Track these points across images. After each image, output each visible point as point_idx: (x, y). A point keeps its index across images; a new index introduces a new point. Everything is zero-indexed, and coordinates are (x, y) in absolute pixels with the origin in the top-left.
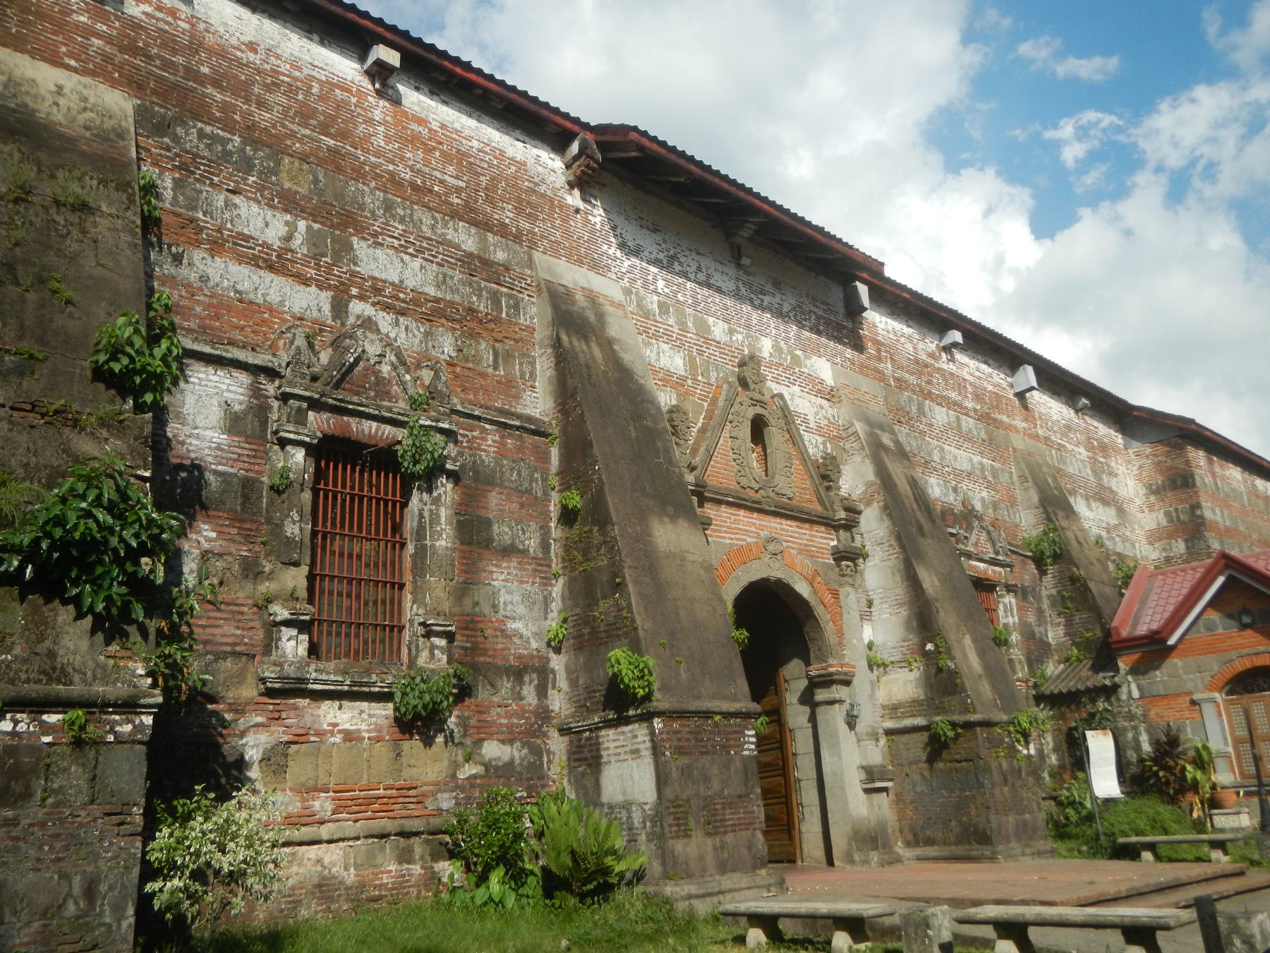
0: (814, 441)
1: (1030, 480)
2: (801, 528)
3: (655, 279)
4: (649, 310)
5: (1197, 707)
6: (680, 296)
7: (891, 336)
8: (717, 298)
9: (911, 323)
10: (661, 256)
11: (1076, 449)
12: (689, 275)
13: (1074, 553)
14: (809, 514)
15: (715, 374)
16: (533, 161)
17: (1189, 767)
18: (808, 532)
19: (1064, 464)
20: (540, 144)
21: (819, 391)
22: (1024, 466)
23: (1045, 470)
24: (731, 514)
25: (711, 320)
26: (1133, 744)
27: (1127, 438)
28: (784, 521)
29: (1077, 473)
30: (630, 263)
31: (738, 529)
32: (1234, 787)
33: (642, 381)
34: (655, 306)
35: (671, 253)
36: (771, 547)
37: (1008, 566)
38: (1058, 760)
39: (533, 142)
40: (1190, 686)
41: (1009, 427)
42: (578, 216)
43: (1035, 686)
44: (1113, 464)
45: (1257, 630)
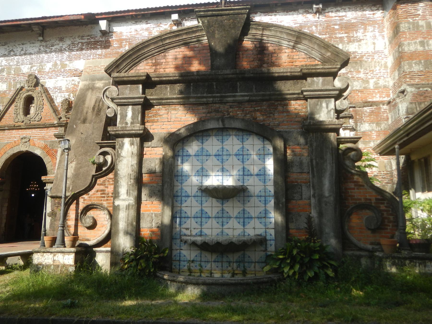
0: (63, 96)
2: (42, 130)
6: (11, 64)
8: (28, 57)
9: (149, 22)
15: (19, 85)
28: (33, 130)
31: (12, 137)
35: (11, 49)
36: (24, 140)
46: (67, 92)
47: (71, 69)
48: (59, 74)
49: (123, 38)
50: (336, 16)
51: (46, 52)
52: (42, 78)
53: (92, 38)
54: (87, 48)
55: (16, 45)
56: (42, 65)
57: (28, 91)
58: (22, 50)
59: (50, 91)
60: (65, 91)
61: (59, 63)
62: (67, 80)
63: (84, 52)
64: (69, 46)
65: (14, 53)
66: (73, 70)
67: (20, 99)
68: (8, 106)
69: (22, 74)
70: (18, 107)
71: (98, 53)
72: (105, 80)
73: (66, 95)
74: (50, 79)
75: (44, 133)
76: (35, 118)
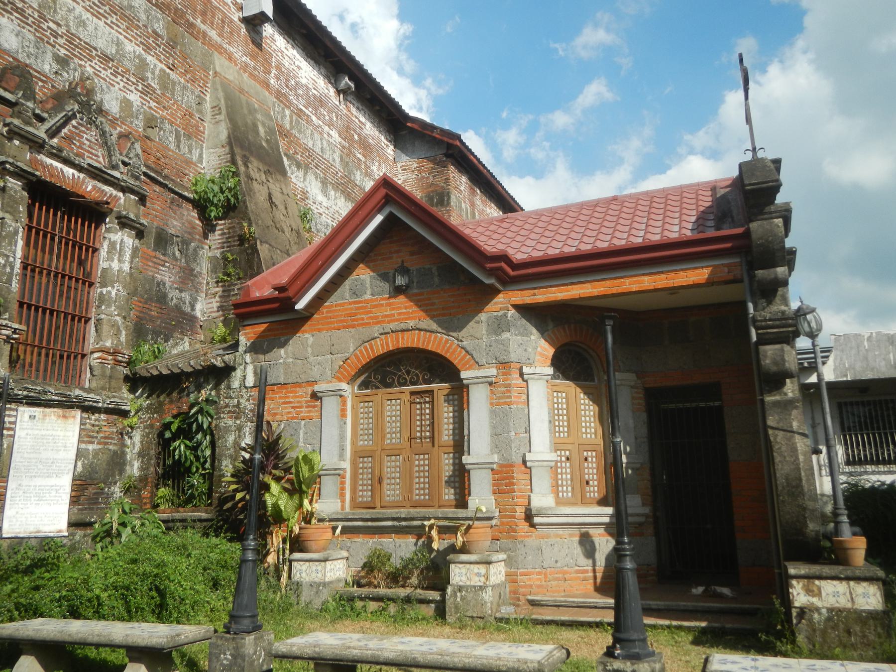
1: (224, 112)
5: (318, 403)
11: (326, 129)
13: (251, 206)
17: (275, 488)
19: (300, 132)
22: (221, 95)
23: (259, 117)
26: (232, 450)
27: (398, 151)
29: (318, 150)
32: (331, 520)
37: (133, 192)
38: (141, 469)
40: (315, 373)
41: (219, 48)
43: (130, 363)
44: (374, 168)
45: (410, 297)
50: (357, 118)
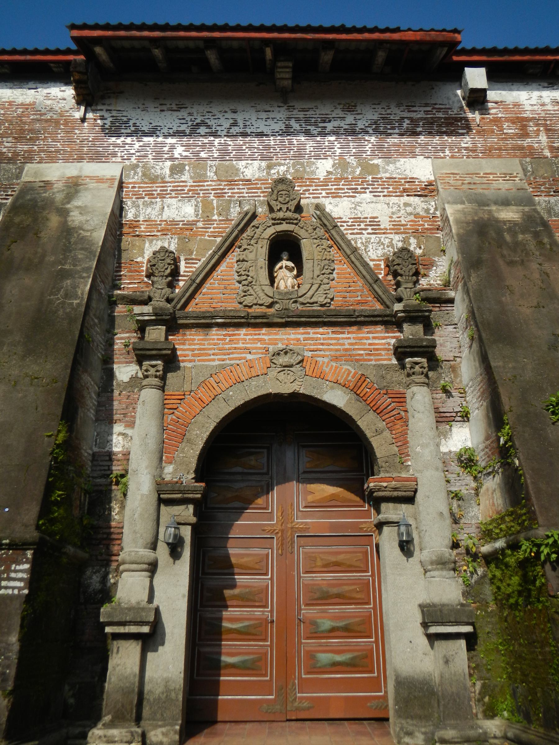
2: (343, 333)
3: (172, 147)
4: (157, 177)
6: (203, 155)
7: (550, 107)
8: (256, 143)
10: (183, 127)
12: (219, 133)
14: (350, 316)
15: (238, 209)
16: (42, 98)
18: (354, 335)
20: (52, 84)
21: (405, 190)
24: (224, 335)
25: (241, 164)
28: (310, 330)
30: (141, 144)
31: (235, 348)
33: (89, 234)
34: (167, 171)
35: (198, 121)
36: (283, 360)
39: (45, 86)
42: (86, 124)
46: (396, 233)
47: (394, 176)
48: (359, 187)
49: (525, 115)
51: (307, 133)
52: (307, 195)
53: (439, 110)
54: (430, 133)
55: (215, 111)
56: (302, 164)
57: (277, 221)
58: (235, 124)
59: (342, 228)
60: (390, 229)
61: (352, 160)
62: (388, 204)
63: (422, 139)
64: (375, 123)
65: (208, 130)
66: (403, 181)
67: (253, 242)
68: (217, 257)
69: (242, 181)
70: (249, 264)
71: (463, 145)
72: (516, 205)
73: (397, 241)
74: (333, 197)
75: (349, 341)
76: (313, 295)
